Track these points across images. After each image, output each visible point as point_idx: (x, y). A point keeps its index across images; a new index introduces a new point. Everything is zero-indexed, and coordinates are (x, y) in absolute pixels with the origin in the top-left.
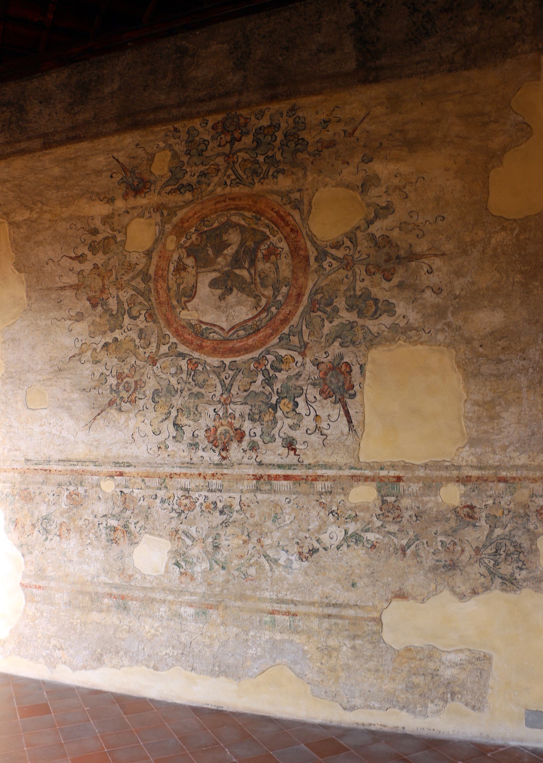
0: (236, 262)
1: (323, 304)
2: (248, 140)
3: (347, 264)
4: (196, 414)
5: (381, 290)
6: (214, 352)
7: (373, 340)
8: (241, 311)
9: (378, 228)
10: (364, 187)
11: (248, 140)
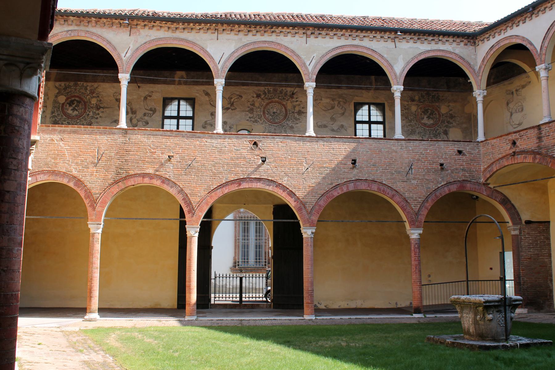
0: (430, 114)
1: (443, 122)
2: (431, 97)
3: (446, 117)
4: (425, 136)
5: (451, 121)
6: (427, 127)
7: (450, 127)
8: (431, 122)
9: (450, 112)
10: (449, 106)
11: (431, 97)
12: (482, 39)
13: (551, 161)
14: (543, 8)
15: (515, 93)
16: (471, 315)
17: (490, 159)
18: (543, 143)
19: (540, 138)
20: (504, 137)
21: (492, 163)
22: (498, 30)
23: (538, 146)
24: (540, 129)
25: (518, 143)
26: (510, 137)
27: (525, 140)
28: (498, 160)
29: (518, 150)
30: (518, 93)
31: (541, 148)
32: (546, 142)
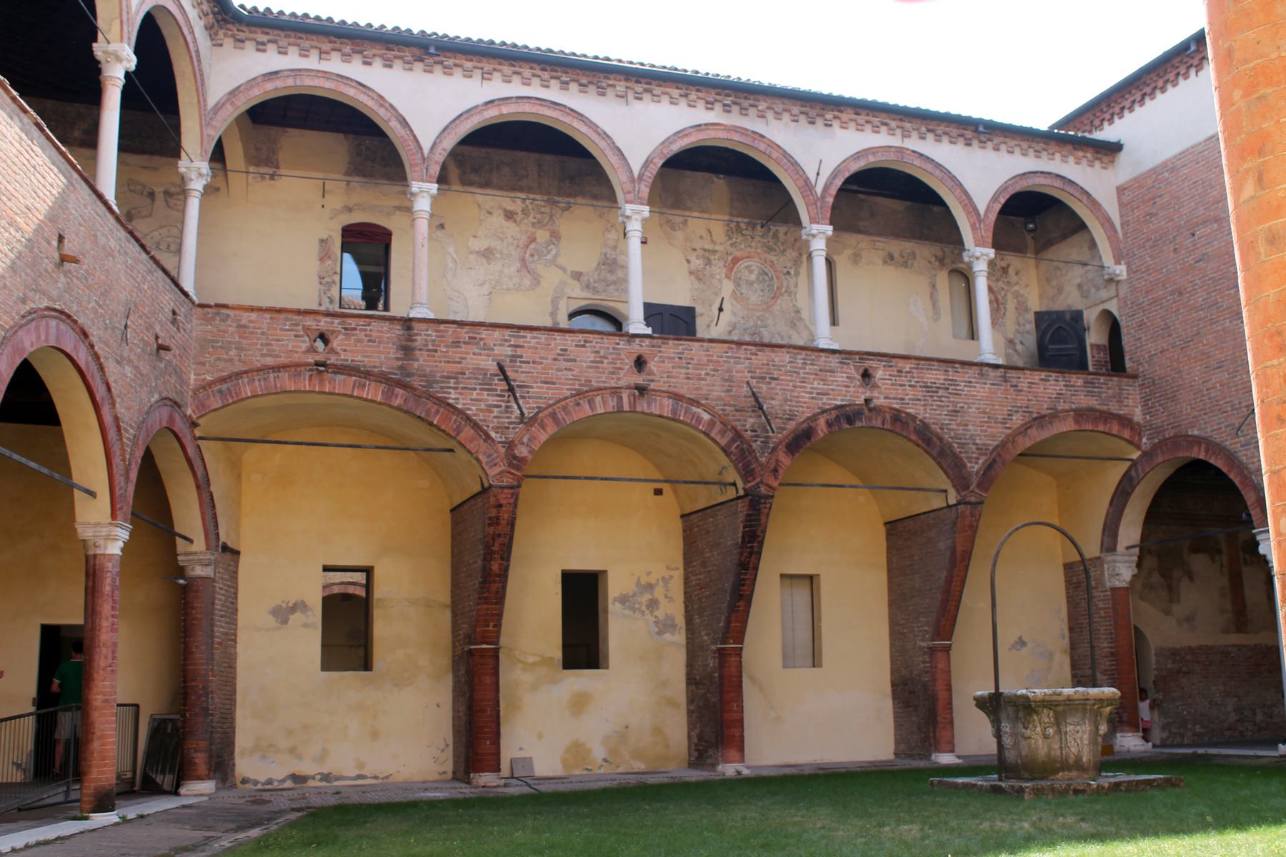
12: (241, 36)
13: (438, 412)
14: (450, 62)
15: (160, 197)
16: (1087, 727)
17: (231, 360)
18: (416, 364)
19: (407, 350)
20: (290, 316)
21: (239, 375)
22: (307, 44)
23: (402, 368)
24: (409, 328)
25: (335, 343)
26: (310, 322)
27: (359, 341)
28: (259, 370)
29: (333, 360)
30: (172, 202)
31: (409, 375)
32: (422, 361)
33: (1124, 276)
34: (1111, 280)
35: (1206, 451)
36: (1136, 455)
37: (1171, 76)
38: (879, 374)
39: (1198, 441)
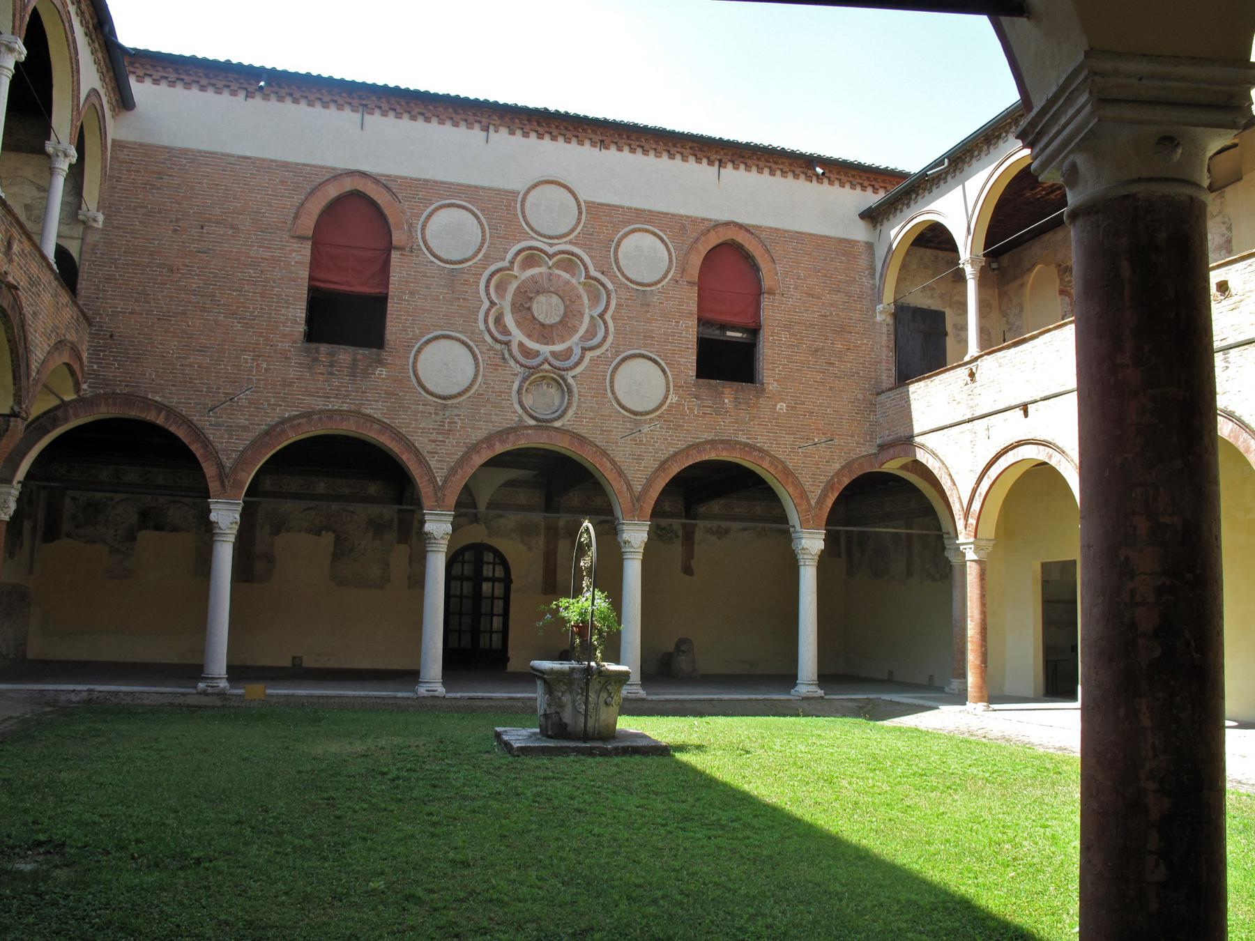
33: (100, 225)
34: (83, 222)
35: (167, 419)
36: (69, 397)
37: (220, 84)
38: (16, 247)
39: (160, 407)
